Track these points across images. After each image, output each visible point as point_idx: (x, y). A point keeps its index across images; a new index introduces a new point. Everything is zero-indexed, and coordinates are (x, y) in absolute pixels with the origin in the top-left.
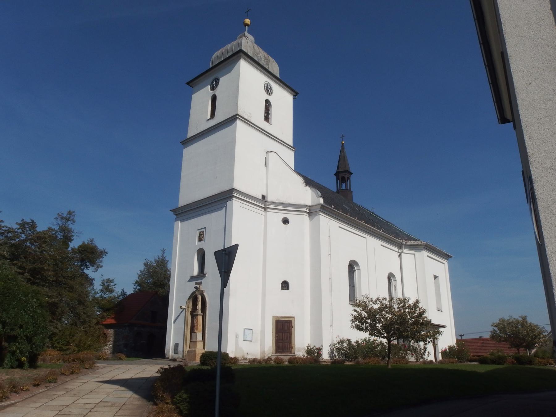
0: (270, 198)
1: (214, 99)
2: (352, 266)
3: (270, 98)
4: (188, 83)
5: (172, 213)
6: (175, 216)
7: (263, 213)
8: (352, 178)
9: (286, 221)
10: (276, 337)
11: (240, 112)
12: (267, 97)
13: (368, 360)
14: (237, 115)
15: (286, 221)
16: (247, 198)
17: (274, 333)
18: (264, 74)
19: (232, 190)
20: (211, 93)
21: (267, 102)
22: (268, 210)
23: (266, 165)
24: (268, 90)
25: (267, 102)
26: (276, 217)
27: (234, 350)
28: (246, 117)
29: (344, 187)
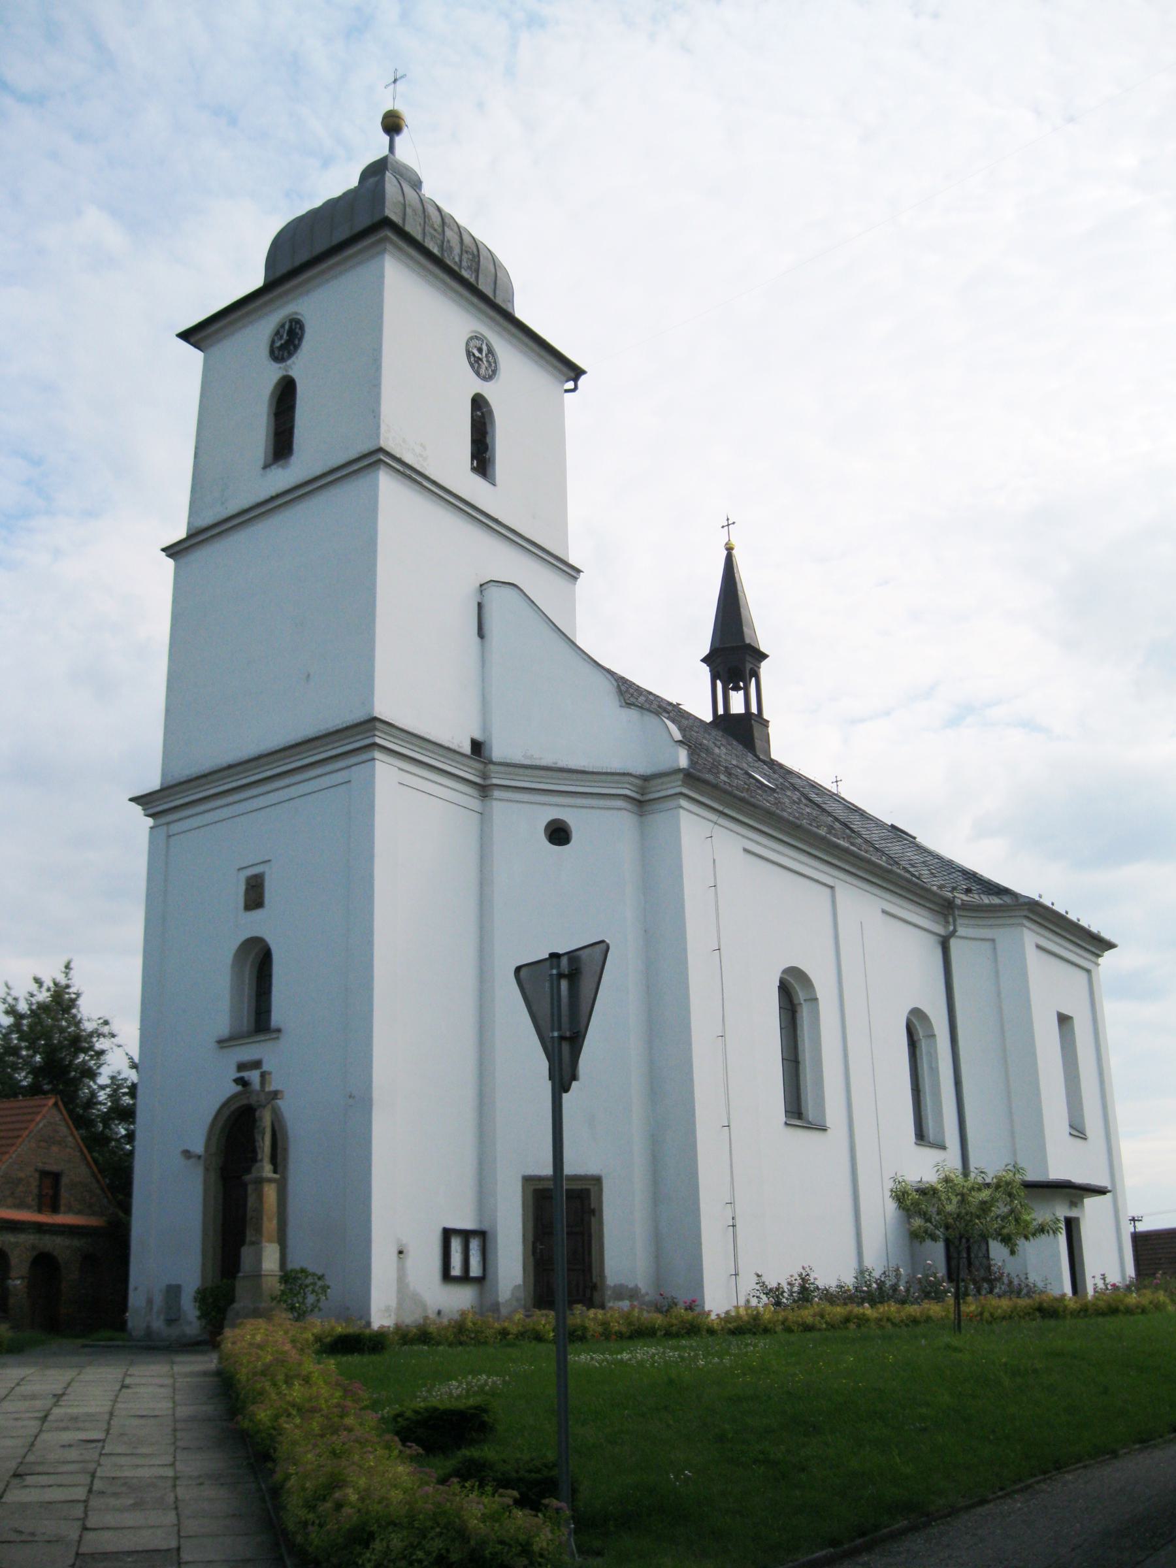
0: (499, 751)
1: (285, 397)
2: (793, 995)
3: (489, 390)
4: (185, 336)
5: (138, 809)
6: (150, 822)
7: (475, 804)
8: (765, 668)
9: (558, 834)
10: (534, 1253)
11: (390, 440)
12: (478, 386)
13: (882, 1308)
14: (381, 450)
15: (558, 834)
16: (420, 752)
17: (531, 1238)
18: (484, 313)
19: (371, 723)
20: (272, 374)
21: (479, 404)
22: (497, 793)
23: (481, 633)
24: (481, 361)
25: (479, 404)
26: (520, 821)
27: (393, 1304)
28: (409, 459)
29: (737, 705)
